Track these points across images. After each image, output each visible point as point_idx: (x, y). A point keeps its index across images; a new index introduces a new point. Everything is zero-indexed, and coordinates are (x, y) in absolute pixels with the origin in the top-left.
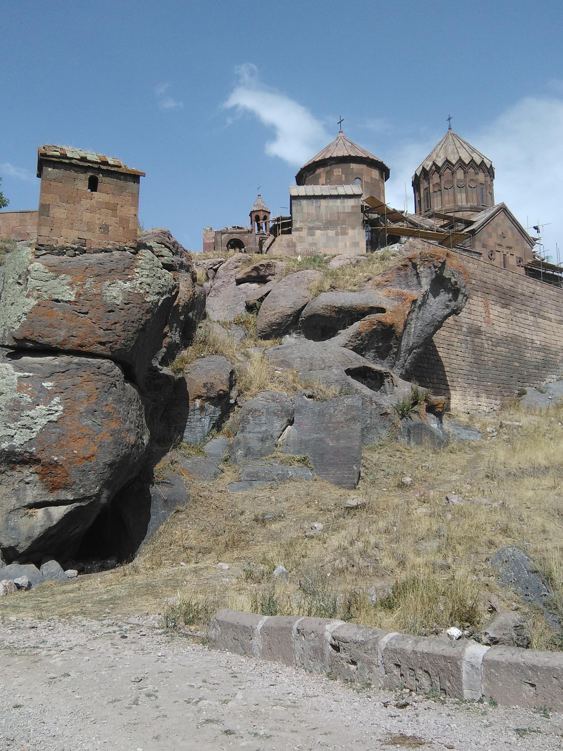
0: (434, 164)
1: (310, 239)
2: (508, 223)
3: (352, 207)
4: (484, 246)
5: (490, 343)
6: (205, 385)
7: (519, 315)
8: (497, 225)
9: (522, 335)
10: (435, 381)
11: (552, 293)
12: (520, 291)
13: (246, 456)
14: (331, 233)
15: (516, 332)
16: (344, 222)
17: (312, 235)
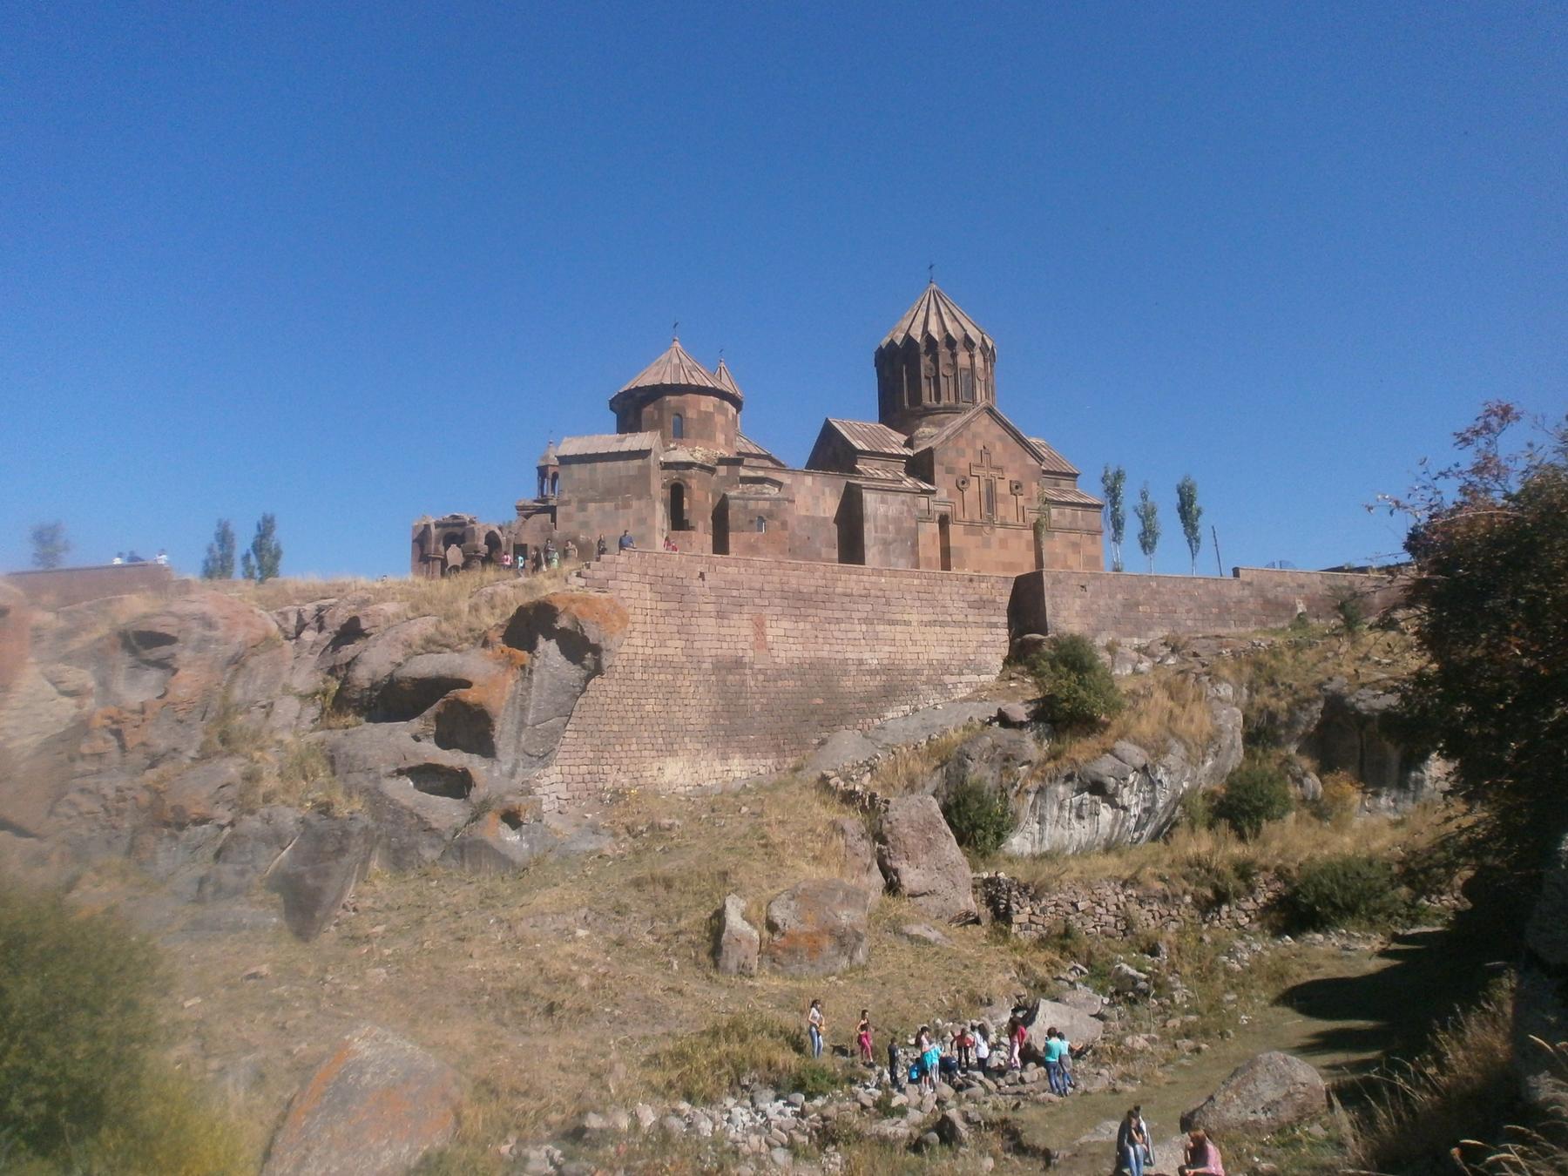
0: (892, 341)
1: (580, 516)
2: (998, 430)
3: (640, 467)
4: (950, 471)
5: (761, 677)
6: (173, 809)
7: (832, 627)
8: (975, 436)
9: (839, 656)
10: (634, 747)
11: (916, 582)
12: (839, 590)
13: (215, 892)
14: (609, 506)
15: (825, 654)
16: (627, 490)
17: (583, 509)
